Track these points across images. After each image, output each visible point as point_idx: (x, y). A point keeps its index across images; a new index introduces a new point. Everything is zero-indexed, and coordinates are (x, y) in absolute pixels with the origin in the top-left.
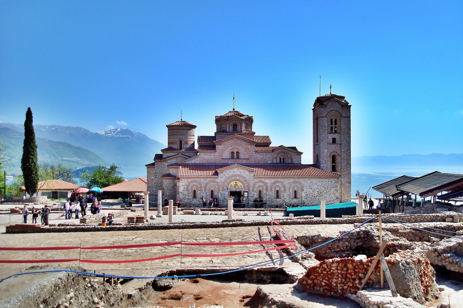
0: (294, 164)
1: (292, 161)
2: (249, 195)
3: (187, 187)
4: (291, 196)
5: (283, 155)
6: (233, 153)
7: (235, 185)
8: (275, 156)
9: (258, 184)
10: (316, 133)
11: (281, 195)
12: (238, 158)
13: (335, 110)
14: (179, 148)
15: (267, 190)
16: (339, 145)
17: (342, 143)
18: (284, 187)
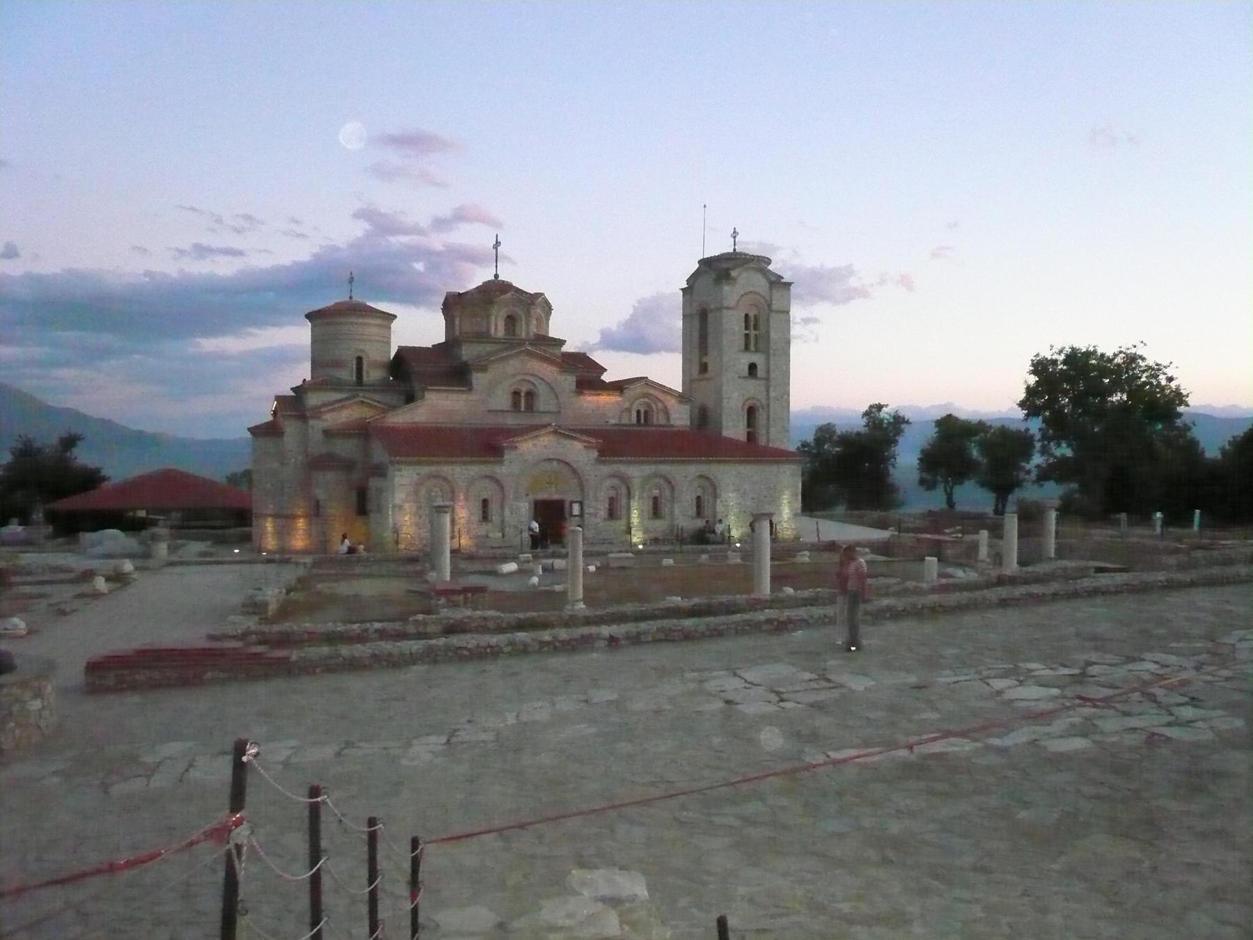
0: (672, 426)
1: (668, 419)
2: (586, 510)
3: (416, 493)
4: (690, 513)
5: (648, 405)
6: (516, 394)
7: (548, 483)
8: (627, 405)
9: (609, 483)
10: (697, 351)
11: (665, 510)
12: (530, 408)
13: (755, 293)
14: (354, 378)
15: (629, 495)
16: (764, 382)
17: (772, 375)
18: (673, 489)
